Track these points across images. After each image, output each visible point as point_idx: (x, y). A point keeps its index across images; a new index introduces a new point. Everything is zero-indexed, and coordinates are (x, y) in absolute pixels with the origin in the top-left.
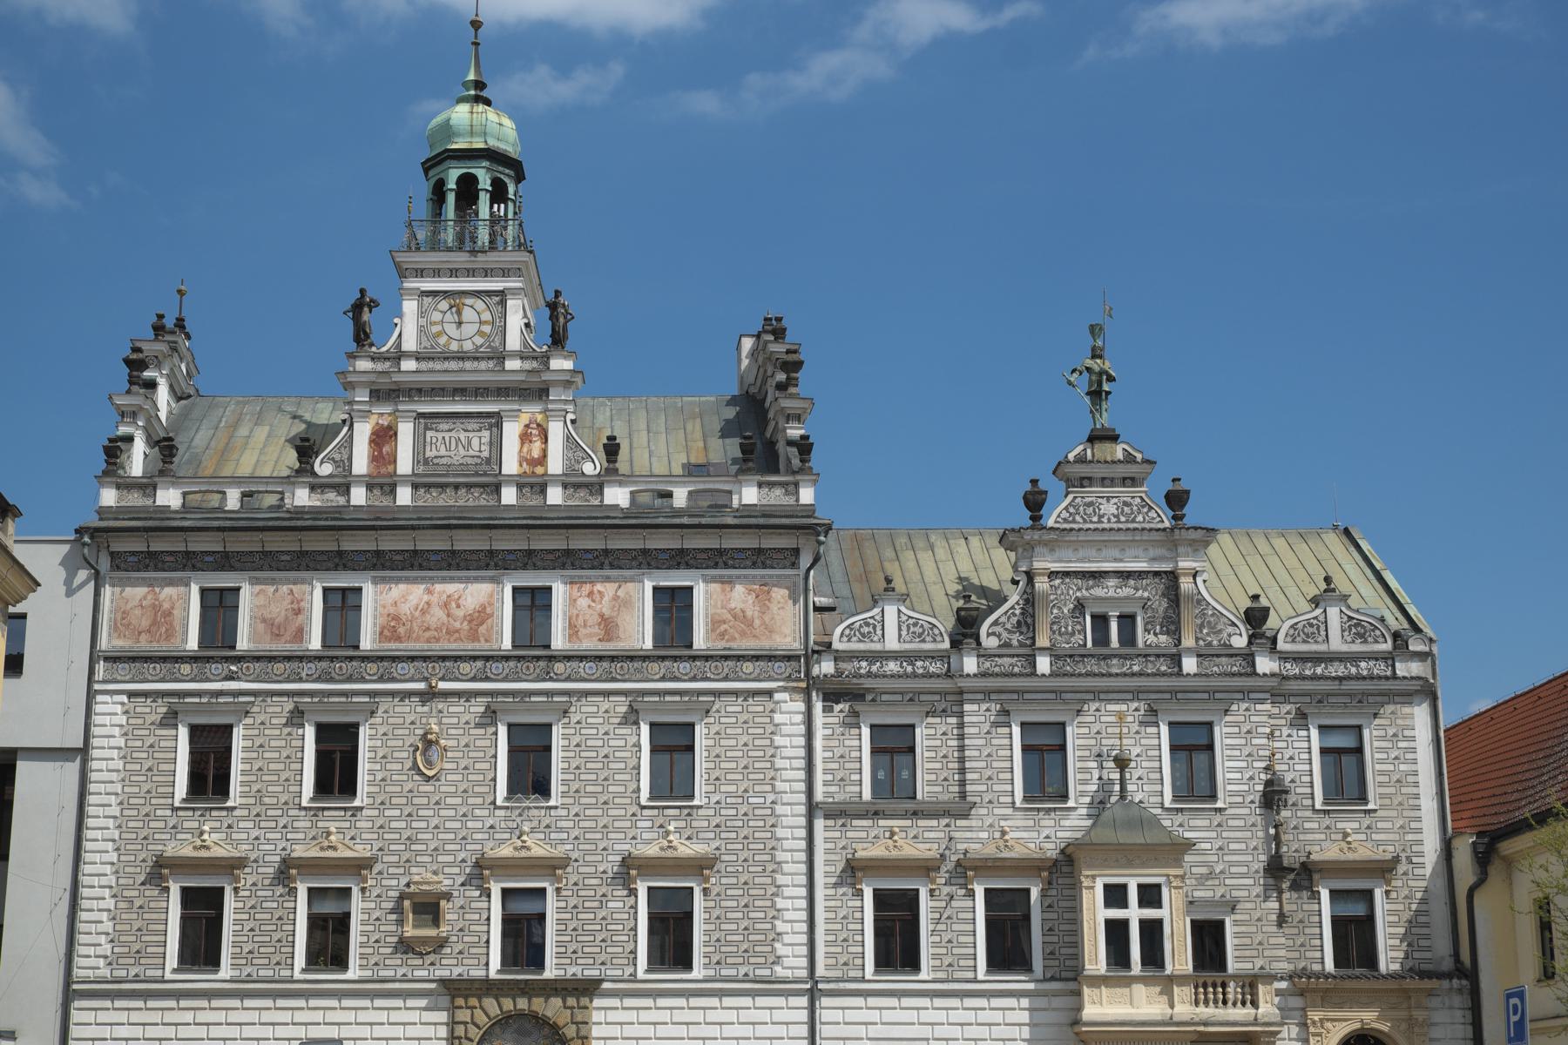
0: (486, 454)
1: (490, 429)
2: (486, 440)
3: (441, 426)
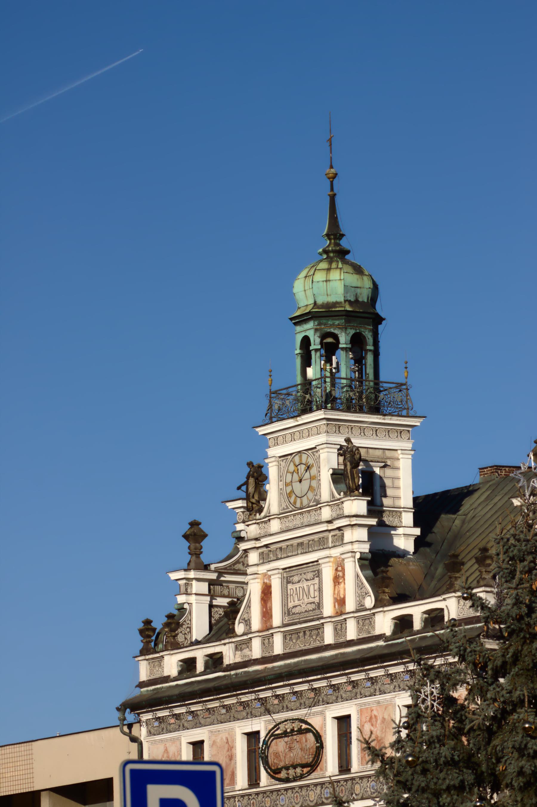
0: (317, 600)
1: (318, 576)
2: (317, 587)
3: (296, 579)
